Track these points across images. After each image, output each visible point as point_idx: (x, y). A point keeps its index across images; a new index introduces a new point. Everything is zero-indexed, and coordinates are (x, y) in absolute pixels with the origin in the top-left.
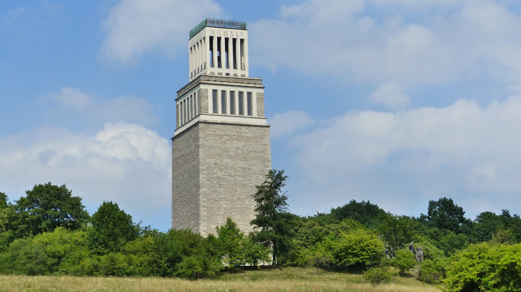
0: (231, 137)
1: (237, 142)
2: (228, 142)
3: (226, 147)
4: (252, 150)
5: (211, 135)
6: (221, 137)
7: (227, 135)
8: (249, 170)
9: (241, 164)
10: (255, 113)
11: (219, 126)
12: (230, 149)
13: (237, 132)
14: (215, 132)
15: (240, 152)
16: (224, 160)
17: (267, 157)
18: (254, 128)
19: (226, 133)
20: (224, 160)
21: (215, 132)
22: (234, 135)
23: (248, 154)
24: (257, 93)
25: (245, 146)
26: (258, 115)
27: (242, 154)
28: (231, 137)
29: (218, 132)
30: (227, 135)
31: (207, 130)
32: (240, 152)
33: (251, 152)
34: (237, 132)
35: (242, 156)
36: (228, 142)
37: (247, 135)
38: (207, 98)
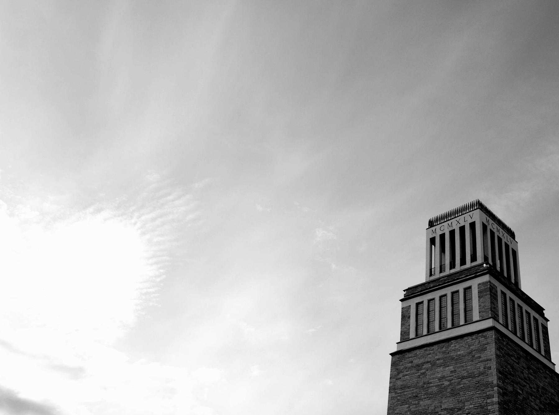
0: (433, 364)
1: (441, 369)
2: (428, 373)
3: (426, 381)
4: (466, 374)
5: (406, 368)
6: (419, 367)
7: (428, 362)
8: (459, 409)
9: (449, 403)
10: (476, 316)
11: (418, 352)
12: (431, 383)
13: (444, 353)
14: (412, 362)
15: (447, 383)
16: (421, 403)
17: (490, 379)
18: (469, 339)
19: (427, 360)
20: (421, 403)
21: (412, 362)
22: (438, 359)
23: (459, 384)
24: (479, 285)
25: (455, 371)
26: (480, 316)
27: (449, 386)
28: (433, 364)
29: (416, 362)
30: (428, 362)
31: (401, 363)
32: (447, 383)
33: (463, 378)
34: (444, 353)
35: (449, 390)
36: (428, 373)
37: (459, 353)
38: (409, 317)
